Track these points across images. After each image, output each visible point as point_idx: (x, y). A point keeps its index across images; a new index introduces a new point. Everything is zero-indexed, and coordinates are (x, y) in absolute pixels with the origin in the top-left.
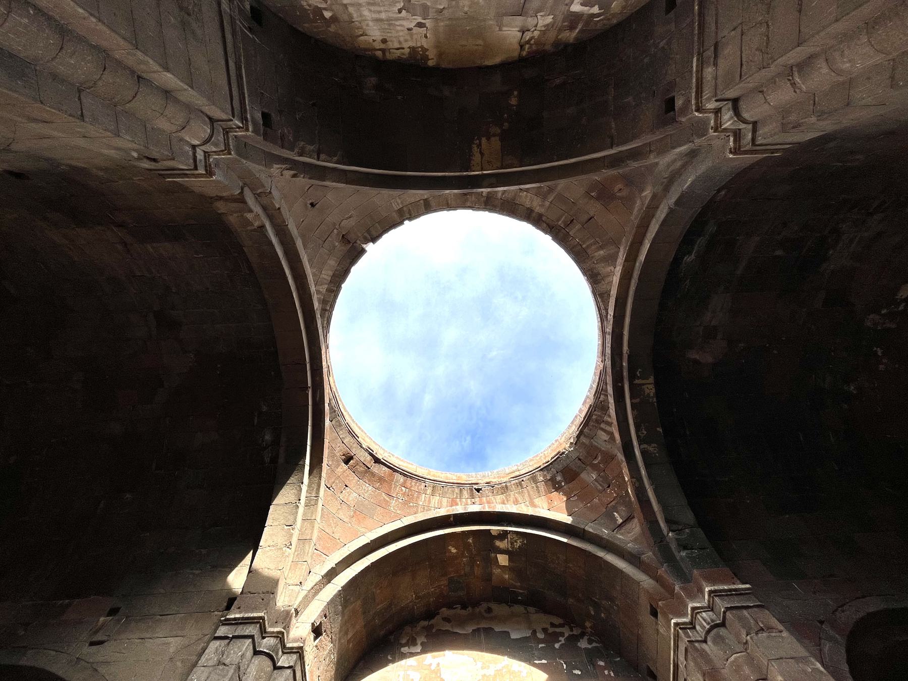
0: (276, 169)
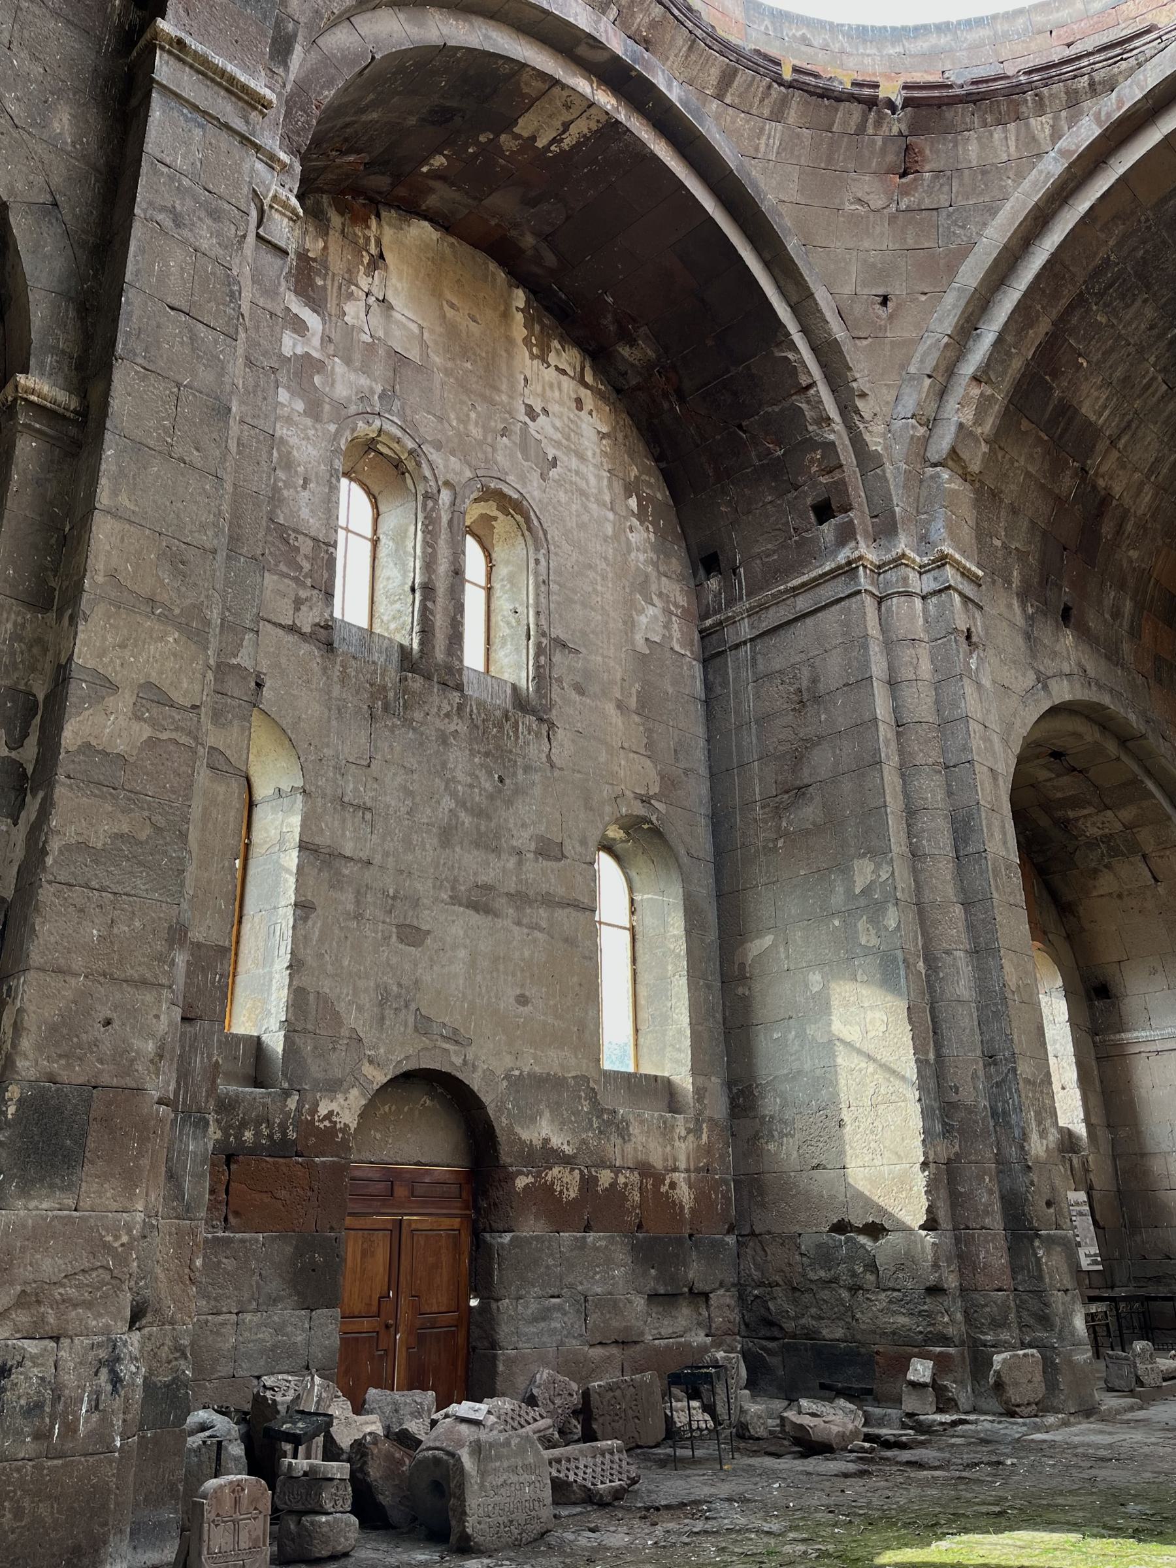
0: (875, 442)
